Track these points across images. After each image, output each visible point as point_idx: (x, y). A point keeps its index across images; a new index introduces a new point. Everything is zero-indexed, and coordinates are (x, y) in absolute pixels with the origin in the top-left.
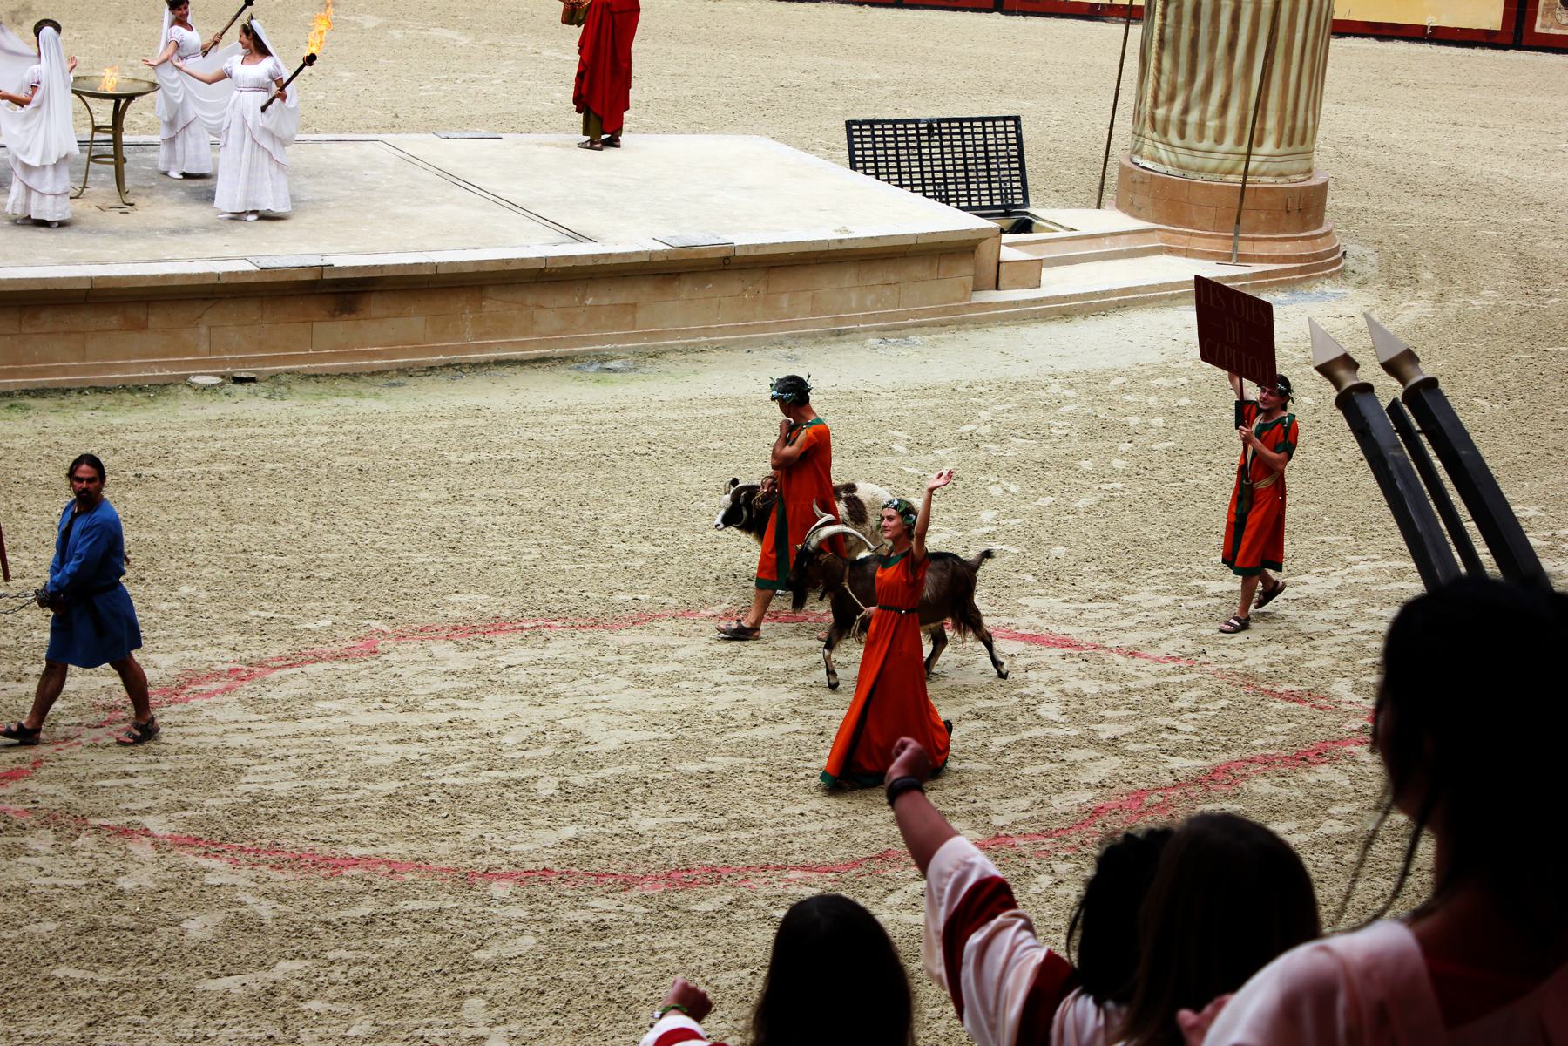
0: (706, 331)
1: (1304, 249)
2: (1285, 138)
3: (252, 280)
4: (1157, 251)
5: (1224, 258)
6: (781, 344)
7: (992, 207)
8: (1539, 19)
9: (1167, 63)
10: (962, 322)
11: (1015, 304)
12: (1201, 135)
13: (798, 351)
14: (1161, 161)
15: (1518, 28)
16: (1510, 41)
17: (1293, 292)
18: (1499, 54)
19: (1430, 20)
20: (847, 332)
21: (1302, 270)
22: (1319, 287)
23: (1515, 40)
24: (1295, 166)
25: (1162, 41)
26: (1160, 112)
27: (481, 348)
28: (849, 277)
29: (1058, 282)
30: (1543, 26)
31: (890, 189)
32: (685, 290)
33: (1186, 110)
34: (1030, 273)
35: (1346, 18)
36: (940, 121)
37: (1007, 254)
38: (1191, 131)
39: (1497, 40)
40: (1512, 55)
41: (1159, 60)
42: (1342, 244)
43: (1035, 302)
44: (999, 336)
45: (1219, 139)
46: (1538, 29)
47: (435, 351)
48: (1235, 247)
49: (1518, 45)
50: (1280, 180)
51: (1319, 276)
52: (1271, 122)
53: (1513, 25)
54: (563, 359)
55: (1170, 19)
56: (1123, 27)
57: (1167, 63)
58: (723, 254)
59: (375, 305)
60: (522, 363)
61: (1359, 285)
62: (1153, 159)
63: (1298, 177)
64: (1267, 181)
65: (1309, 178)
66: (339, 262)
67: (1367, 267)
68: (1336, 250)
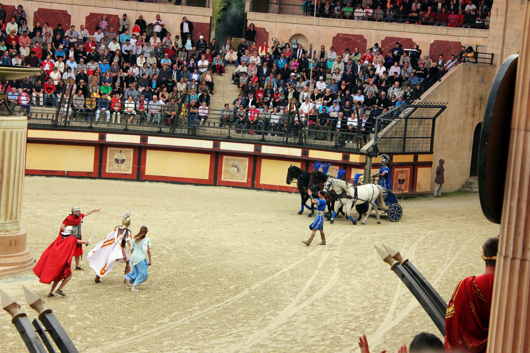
1: (19, 260)
8: (107, 167)
15: (100, 171)
16: (96, 176)
17: (15, 277)
18: (93, 181)
19: (66, 169)
21: (18, 268)
23: (99, 175)
24: (14, 227)
30: (109, 170)
35: (34, 169)
42: (34, 257)
46: (107, 171)
50: (7, 233)
51: (25, 271)
53: (98, 170)
63: (15, 232)
65: (19, 232)
68: (32, 259)
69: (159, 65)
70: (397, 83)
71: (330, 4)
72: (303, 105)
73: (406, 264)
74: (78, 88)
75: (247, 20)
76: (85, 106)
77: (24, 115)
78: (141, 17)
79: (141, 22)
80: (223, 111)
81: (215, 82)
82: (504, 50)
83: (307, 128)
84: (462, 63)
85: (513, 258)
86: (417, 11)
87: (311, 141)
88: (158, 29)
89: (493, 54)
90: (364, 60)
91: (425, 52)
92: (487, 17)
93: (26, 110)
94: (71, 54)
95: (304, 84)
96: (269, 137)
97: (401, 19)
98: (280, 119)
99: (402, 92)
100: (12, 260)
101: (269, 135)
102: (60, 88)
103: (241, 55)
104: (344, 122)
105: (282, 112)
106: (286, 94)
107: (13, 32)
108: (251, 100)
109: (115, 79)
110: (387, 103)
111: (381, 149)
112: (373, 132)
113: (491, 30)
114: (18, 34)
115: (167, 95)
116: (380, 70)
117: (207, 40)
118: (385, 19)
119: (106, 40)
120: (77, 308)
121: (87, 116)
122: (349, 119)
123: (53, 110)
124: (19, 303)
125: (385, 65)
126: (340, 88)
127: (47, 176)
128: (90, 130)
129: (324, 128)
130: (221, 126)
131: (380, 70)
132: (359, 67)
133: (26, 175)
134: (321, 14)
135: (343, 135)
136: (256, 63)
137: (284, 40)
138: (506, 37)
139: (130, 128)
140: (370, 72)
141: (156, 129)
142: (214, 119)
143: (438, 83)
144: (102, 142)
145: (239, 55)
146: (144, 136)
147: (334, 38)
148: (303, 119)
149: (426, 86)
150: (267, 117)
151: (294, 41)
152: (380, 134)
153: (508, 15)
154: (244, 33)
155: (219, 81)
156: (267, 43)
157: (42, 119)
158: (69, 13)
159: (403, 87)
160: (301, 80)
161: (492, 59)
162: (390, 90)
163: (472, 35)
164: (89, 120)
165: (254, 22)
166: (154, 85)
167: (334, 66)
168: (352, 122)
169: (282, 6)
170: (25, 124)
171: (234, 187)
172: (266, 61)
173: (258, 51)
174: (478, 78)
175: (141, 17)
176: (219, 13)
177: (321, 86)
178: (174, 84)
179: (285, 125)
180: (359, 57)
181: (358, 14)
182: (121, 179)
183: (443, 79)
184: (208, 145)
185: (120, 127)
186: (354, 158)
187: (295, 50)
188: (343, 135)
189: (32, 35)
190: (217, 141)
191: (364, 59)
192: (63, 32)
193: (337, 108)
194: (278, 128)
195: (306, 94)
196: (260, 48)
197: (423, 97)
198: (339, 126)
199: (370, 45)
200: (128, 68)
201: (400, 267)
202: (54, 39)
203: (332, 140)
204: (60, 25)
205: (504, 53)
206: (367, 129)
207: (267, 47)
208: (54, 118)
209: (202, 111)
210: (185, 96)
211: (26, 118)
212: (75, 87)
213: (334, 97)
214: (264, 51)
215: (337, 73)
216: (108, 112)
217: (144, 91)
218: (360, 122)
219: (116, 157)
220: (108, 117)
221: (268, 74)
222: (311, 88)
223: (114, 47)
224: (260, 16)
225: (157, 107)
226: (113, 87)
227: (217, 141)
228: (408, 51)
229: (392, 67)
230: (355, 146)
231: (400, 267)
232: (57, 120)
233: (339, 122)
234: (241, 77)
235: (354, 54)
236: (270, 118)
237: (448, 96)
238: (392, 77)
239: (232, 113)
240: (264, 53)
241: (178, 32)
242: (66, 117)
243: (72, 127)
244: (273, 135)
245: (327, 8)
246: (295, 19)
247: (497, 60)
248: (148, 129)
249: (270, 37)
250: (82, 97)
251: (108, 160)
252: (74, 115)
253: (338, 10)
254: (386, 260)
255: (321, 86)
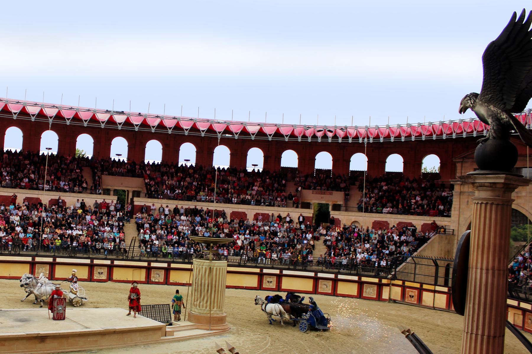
0: (111, 345)
1: (223, 328)
2: (218, 307)
3: (25, 336)
4: (196, 329)
5: (207, 330)
6: (125, 347)
7: (165, 321)
9: (196, 294)
10: (159, 343)
11: (169, 339)
12: (203, 307)
13: (128, 349)
14: (196, 312)
17: (221, 336)
19: (244, 285)
20: (138, 345)
22: (226, 335)
25: (195, 290)
26: (195, 303)
27: (68, 349)
28: (138, 334)
29: (177, 335)
31: (146, 318)
32: (107, 337)
33: (200, 303)
34: (172, 334)
36: (155, 305)
37: (167, 330)
38: (201, 306)
39: (256, 289)
40: (259, 291)
41: (195, 293)
43: (173, 339)
44: (166, 345)
45: (206, 308)
46: (264, 287)
47: (59, 350)
48: (210, 328)
49: (260, 289)
52: (215, 305)
54: (83, 351)
55: (196, 286)
56: (188, 287)
57: (196, 294)
58: (113, 331)
59: (48, 341)
60: (75, 351)
61: (233, 334)
62: (194, 312)
64: (215, 315)
66: (41, 333)
67: (234, 331)
69: (288, 237)
70: (405, 244)
71: (371, 206)
72: (358, 254)
73: (413, 335)
74: (250, 248)
75: (330, 215)
76: (253, 256)
77: (226, 260)
78: (279, 214)
79: (279, 217)
80: (319, 258)
81: (315, 245)
82: (459, 227)
83: (360, 266)
84: (438, 234)
85: (472, 334)
86: (414, 209)
87: (363, 273)
88: (288, 219)
89: (453, 230)
90: (388, 233)
91: (419, 229)
92: (450, 212)
93: (226, 258)
94: (248, 232)
95: (358, 245)
96: (342, 271)
97: (407, 213)
98: (347, 262)
99: (408, 249)
100: (219, 328)
101: (342, 269)
102: (242, 248)
103: (328, 232)
104: (379, 263)
105: (348, 258)
106: (350, 250)
107: (221, 222)
108: (333, 253)
109: (267, 243)
110: (400, 253)
111: (398, 277)
112: (394, 268)
113: (452, 218)
114: (223, 223)
115: (292, 250)
116: (396, 238)
117: (311, 224)
118: (398, 213)
119: (263, 225)
120: (250, 351)
121: (255, 260)
122: (382, 262)
123: (239, 258)
124: (223, 348)
125: (398, 235)
126: (376, 247)
127: (236, 289)
128: (256, 267)
129: (369, 266)
130: (318, 266)
131: (396, 238)
132: (386, 236)
133: (226, 288)
134: (366, 211)
135: (378, 270)
136: (335, 235)
137: (348, 224)
138: (460, 221)
139: (275, 266)
140: (391, 239)
141: (287, 267)
142: (315, 262)
143: (426, 244)
144: (261, 273)
145: (327, 232)
146: (281, 270)
147: (373, 223)
148: (358, 262)
149: (419, 246)
150: (341, 261)
151: (353, 224)
152: (397, 269)
153: (461, 210)
154: (329, 221)
155: (317, 244)
156: (340, 225)
157: (234, 262)
158: (246, 213)
159: (408, 246)
160: (357, 243)
161: (453, 232)
162: (402, 248)
163: (442, 220)
164: (256, 263)
165: (333, 216)
166: (286, 246)
167: (373, 236)
168: (383, 263)
169: (347, 208)
170: (226, 264)
171: (325, 295)
172: (340, 234)
173: (335, 229)
174: (446, 242)
175: (279, 214)
176: (317, 212)
177: (367, 246)
178: (296, 246)
179: (350, 265)
180: (386, 231)
181: (384, 211)
182: (270, 291)
183: (429, 242)
184: (312, 274)
185: (270, 266)
186: (384, 281)
187: (354, 229)
188: (378, 270)
189: (229, 223)
190: (316, 272)
191: (388, 232)
192: (243, 222)
193: (375, 256)
194: (346, 267)
195: (360, 250)
196: (337, 228)
197: (418, 251)
198: (376, 265)
199: (391, 226)
200: (274, 238)
201: (410, 336)
202: (239, 225)
203: (373, 272)
204: (242, 218)
205: (459, 229)
206: (391, 267)
207: (340, 227)
208: (239, 262)
209: (310, 258)
210: (300, 251)
211: (226, 261)
212: (249, 247)
213: (374, 251)
214: (339, 230)
215: (375, 240)
216: (264, 259)
217: (281, 249)
218: (387, 263)
219: (268, 280)
220: (264, 261)
221: (341, 240)
222: (362, 247)
223: (266, 228)
224: (337, 213)
225: (287, 256)
226: (267, 247)
227: (316, 272)
228: (410, 229)
229: (402, 236)
230: (385, 275)
231: (410, 336)
232: (240, 262)
233: (377, 264)
234: (328, 242)
235: (383, 230)
236: (342, 262)
237: (431, 250)
238: (403, 241)
239: (324, 259)
240: (339, 231)
241: (297, 221)
242: (245, 261)
243: (247, 266)
244: (344, 270)
245: (369, 208)
246: (353, 214)
247: (456, 233)
248: (284, 267)
249: (342, 223)
250: (252, 252)
251: (264, 282)
252: (248, 260)
253: (375, 209)
254: (403, 333)
255: (367, 246)
